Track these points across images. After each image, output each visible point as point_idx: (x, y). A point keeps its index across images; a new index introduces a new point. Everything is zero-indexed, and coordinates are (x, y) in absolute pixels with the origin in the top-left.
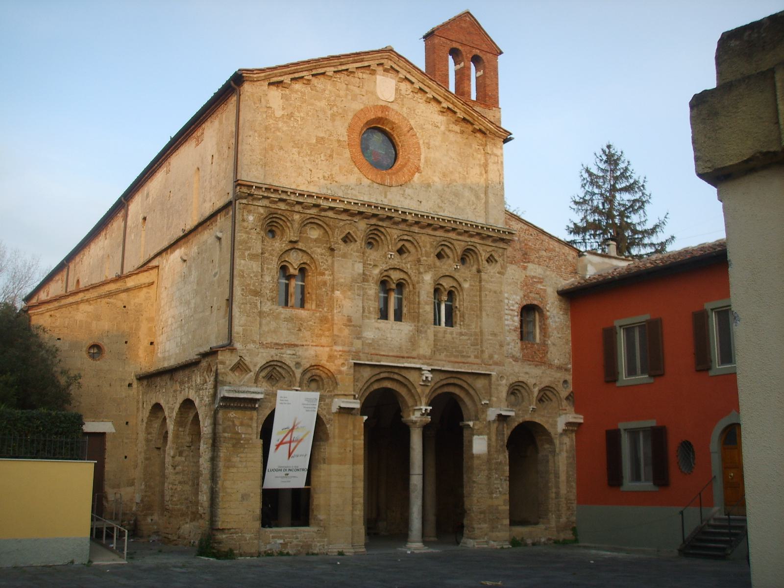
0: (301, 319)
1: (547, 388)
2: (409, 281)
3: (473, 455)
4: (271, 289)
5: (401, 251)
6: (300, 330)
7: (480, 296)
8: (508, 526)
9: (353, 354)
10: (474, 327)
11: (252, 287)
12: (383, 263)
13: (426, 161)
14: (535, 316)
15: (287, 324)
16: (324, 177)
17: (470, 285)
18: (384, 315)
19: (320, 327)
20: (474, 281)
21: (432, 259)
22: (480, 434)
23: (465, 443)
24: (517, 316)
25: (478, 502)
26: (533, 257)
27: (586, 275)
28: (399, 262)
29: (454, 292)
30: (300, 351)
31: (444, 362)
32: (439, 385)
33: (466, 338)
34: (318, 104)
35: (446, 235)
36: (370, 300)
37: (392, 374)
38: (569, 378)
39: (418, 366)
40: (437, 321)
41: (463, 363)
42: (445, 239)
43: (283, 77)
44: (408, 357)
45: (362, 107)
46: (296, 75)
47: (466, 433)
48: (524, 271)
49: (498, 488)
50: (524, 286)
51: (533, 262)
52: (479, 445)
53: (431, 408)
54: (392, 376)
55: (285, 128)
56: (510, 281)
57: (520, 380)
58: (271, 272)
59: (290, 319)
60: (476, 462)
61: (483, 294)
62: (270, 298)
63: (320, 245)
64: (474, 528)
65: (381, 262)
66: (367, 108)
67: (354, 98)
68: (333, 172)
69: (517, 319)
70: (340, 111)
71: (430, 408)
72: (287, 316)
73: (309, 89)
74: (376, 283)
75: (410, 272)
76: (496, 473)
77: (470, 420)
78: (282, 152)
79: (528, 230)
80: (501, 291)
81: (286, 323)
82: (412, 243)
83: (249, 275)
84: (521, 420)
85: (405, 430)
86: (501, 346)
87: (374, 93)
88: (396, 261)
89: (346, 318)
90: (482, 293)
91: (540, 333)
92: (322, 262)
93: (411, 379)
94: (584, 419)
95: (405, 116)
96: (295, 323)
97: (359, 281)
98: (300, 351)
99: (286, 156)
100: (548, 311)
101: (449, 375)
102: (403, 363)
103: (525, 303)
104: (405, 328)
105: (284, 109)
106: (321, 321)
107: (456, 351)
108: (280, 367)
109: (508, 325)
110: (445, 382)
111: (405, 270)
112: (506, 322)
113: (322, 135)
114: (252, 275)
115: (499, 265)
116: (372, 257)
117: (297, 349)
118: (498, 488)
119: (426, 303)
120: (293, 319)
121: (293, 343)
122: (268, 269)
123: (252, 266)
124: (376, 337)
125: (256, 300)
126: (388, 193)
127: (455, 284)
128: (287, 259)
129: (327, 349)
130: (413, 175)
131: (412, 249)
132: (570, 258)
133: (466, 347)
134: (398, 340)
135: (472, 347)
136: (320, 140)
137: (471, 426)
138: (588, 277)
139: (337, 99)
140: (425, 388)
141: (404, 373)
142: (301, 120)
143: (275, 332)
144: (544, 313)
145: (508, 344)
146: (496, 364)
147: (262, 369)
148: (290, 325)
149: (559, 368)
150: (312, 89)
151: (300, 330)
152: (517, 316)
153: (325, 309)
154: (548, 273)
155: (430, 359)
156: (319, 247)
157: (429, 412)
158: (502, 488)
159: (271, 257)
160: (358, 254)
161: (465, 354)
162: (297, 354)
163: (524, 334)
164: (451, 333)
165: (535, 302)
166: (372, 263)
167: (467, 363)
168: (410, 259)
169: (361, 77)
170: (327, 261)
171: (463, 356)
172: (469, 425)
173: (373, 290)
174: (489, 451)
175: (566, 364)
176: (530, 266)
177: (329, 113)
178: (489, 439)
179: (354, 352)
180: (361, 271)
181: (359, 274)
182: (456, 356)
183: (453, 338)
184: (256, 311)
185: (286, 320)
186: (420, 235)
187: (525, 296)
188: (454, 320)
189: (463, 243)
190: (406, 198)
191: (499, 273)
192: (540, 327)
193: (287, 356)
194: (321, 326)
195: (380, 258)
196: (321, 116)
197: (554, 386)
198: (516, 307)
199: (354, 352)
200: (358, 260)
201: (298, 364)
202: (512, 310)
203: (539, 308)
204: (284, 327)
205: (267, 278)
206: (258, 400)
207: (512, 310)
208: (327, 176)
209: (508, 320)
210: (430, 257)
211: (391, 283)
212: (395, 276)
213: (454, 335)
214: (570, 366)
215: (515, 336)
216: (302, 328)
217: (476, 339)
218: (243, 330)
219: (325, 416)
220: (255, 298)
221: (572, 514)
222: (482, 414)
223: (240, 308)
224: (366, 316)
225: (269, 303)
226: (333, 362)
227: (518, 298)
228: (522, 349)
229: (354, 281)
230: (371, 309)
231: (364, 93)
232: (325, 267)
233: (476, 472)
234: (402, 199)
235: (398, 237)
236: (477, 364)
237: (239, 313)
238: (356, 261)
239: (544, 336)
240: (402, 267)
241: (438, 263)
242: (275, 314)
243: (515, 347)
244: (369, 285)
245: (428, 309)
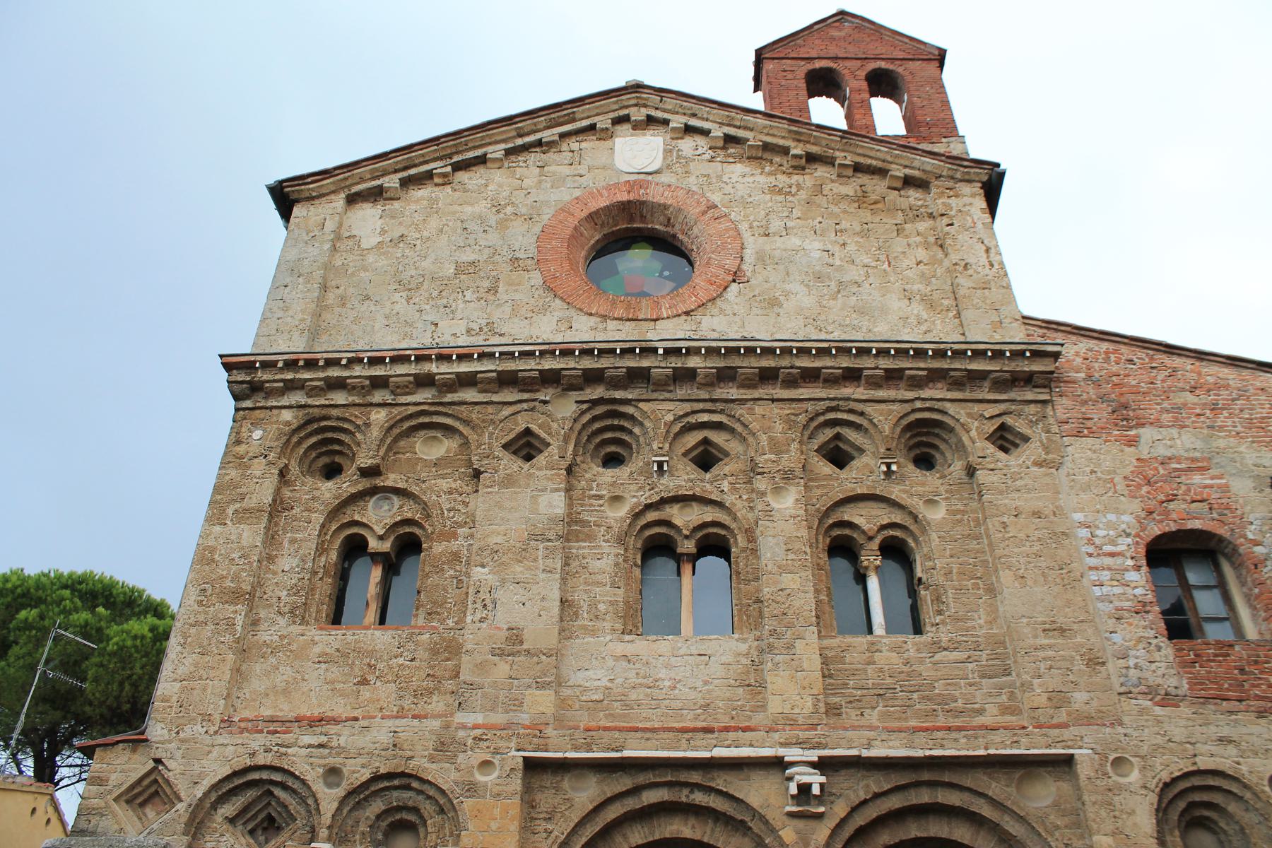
0: (371, 653)
2: (733, 526)
6: (364, 682)
30: (344, 737)
32: (872, 812)
35: (833, 393)
37: (686, 791)
42: (834, 404)
54: (684, 796)
62: (286, 610)
72: (328, 650)
75: (729, 500)
81: (323, 666)
82: (732, 431)
88: (684, 478)
93: (754, 800)
96: (352, 666)
98: (344, 737)
111: (713, 497)
117: (333, 729)
120: (347, 656)
124: (620, 681)
128: (357, 517)
134: (699, 684)
140: (812, 824)
141: (721, 781)
148: (335, 672)
162: (334, 744)
168: (727, 469)
185: (324, 659)
186: (749, 405)
204: (315, 677)
211: (679, 539)
212: (685, 518)
216: (371, 677)
236: (1005, 728)
242: (294, 647)
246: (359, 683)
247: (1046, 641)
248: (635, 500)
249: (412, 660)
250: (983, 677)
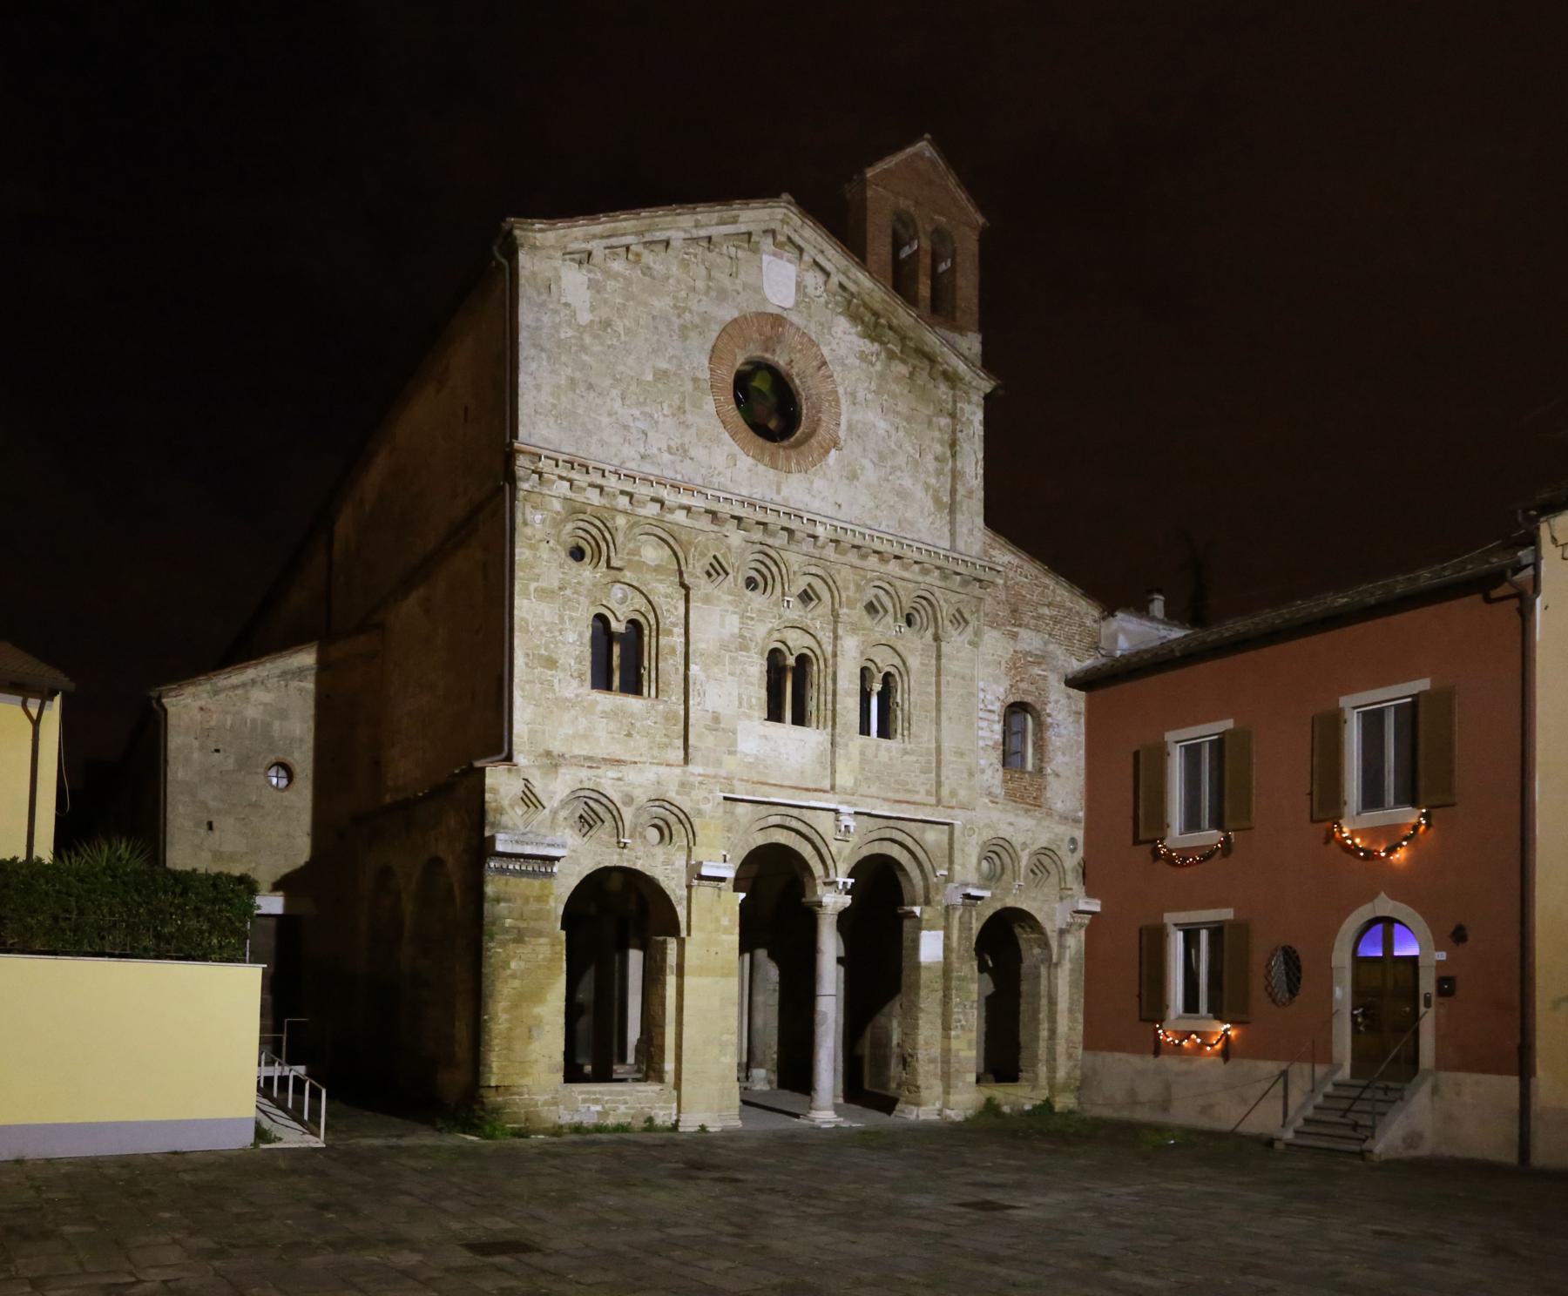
0: (632, 715)
1: (1043, 851)
3: (919, 963)
4: (578, 657)
5: (806, 597)
6: (629, 735)
7: (938, 684)
8: (974, 1084)
9: (723, 780)
10: (926, 739)
11: (543, 652)
12: (775, 617)
14: (1025, 719)
15: (607, 724)
16: (669, 448)
17: (922, 664)
18: (775, 714)
19: (664, 732)
20: (928, 656)
21: (859, 612)
22: (931, 928)
23: (907, 943)
24: (999, 722)
25: (927, 1043)
26: (1026, 619)
27: (1115, 650)
28: (800, 616)
29: (893, 676)
31: (874, 801)
33: (913, 758)
34: (656, 303)
36: (752, 684)
39: (832, 806)
40: (865, 730)
41: (908, 802)
43: (591, 243)
44: (816, 790)
45: (736, 314)
46: (613, 241)
47: (907, 924)
48: (1012, 642)
49: (960, 1021)
50: (1010, 669)
51: (1027, 626)
52: (930, 947)
53: (853, 880)
55: (597, 348)
56: (989, 657)
57: (1000, 836)
58: (576, 624)
59: (613, 714)
60: (924, 975)
61: (944, 679)
63: (662, 577)
64: (918, 1087)
65: (770, 615)
66: (745, 318)
67: (722, 296)
68: (686, 440)
69: (998, 727)
70: (697, 320)
71: (851, 881)
73: (639, 272)
74: (762, 654)
75: (820, 635)
76: (958, 996)
77: (914, 904)
78: (592, 394)
79: (1021, 567)
80: (973, 675)
83: (537, 628)
85: (809, 917)
86: (971, 775)
87: (758, 289)
88: (795, 612)
89: (710, 715)
90: (942, 677)
91: (1033, 755)
92: (668, 611)
94: (1102, 907)
97: (732, 647)
99: (599, 401)
100: (1049, 715)
101: (885, 822)
102: (808, 800)
103: (1011, 700)
104: (810, 739)
105: (593, 309)
106: (667, 719)
107: (896, 781)
109: (983, 738)
110: (875, 835)
112: (981, 733)
113: (664, 365)
114: (543, 629)
115: (970, 629)
116: (755, 605)
118: (960, 1021)
119: (847, 693)
120: (616, 714)
121: (618, 758)
122: (571, 619)
123: (543, 611)
125: (552, 676)
126: (783, 486)
127: (897, 661)
129: (678, 771)
131: (826, 595)
132: (1089, 622)
133: (913, 774)
135: (923, 775)
136: (661, 375)
137: (918, 914)
138: (1118, 653)
139: (691, 295)
142: (626, 334)
143: (585, 737)
144: (1042, 718)
145: (983, 771)
146: (963, 807)
147: (564, 804)
148: (612, 726)
150: (644, 274)
151: (629, 735)
152: (999, 722)
153: (673, 698)
154: (1051, 647)
155: (853, 795)
157: (849, 887)
158: (967, 1021)
160: (731, 598)
161: (910, 787)
163: (1010, 756)
164: (888, 749)
165: (1028, 699)
166: (754, 615)
167: (914, 803)
168: (820, 610)
169: (733, 255)
170: (676, 608)
171: (909, 791)
172: (913, 912)
173: (757, 669)
174: (946, 958)
176: (1023, 633)
177: (676, 322)
178: (947, 937)
179: (725, 778)
180: (736, 630)
181: (732, 635)
182: (898, 791)
183: (891, 759)
184: (550, 696)
185: (605, 714)
187: (1012, 686)
188: (892, 727)
189: (911, 586)
190: (813, 496)
191: (970, 643)
192: (1034, 743)
193: (607, 781)
194: (666, 729)
195: (768, 607)
196: (662, 328)
198: (997, 707)
199: (725, 778)
200: (731, 608)
202: (990, 711)
203: (1033, 708)
204: (602, 729)
205: (571, 637)
206: (558, 859)
207: (990, 711)
208: (674, 447)
209: (982, 729)
210: (855, 608)
213: (894, 753)
215: (995, 757)
217: (929, 762)
218: (530, 731)
220: (550, 673)
221: (1075, 1066)
222: (937, 894)
223: (523, 690)
224: (745, 713)
225: (575, 683)
226: (688, 794)
227: (1000, 690)
228: (1005, 781)
229: (724, 646)
230: (754, 700)
231: (740, 289)
232: (672, 619)
233: (923, 993)
234: (807, 498)
235: (800, 567)
237: (521, 699)
238: (727, 611)
239: (1041, 760)
240: (807, 625)
241: (867, 620)
242: (585, 704)
243: (993, 778)
244: (748, 657)
245: (850, 705)
246: (626, 735)
247: (953, 759)
248: (771, 625)
249: (655, 723)
250: (921, 772)
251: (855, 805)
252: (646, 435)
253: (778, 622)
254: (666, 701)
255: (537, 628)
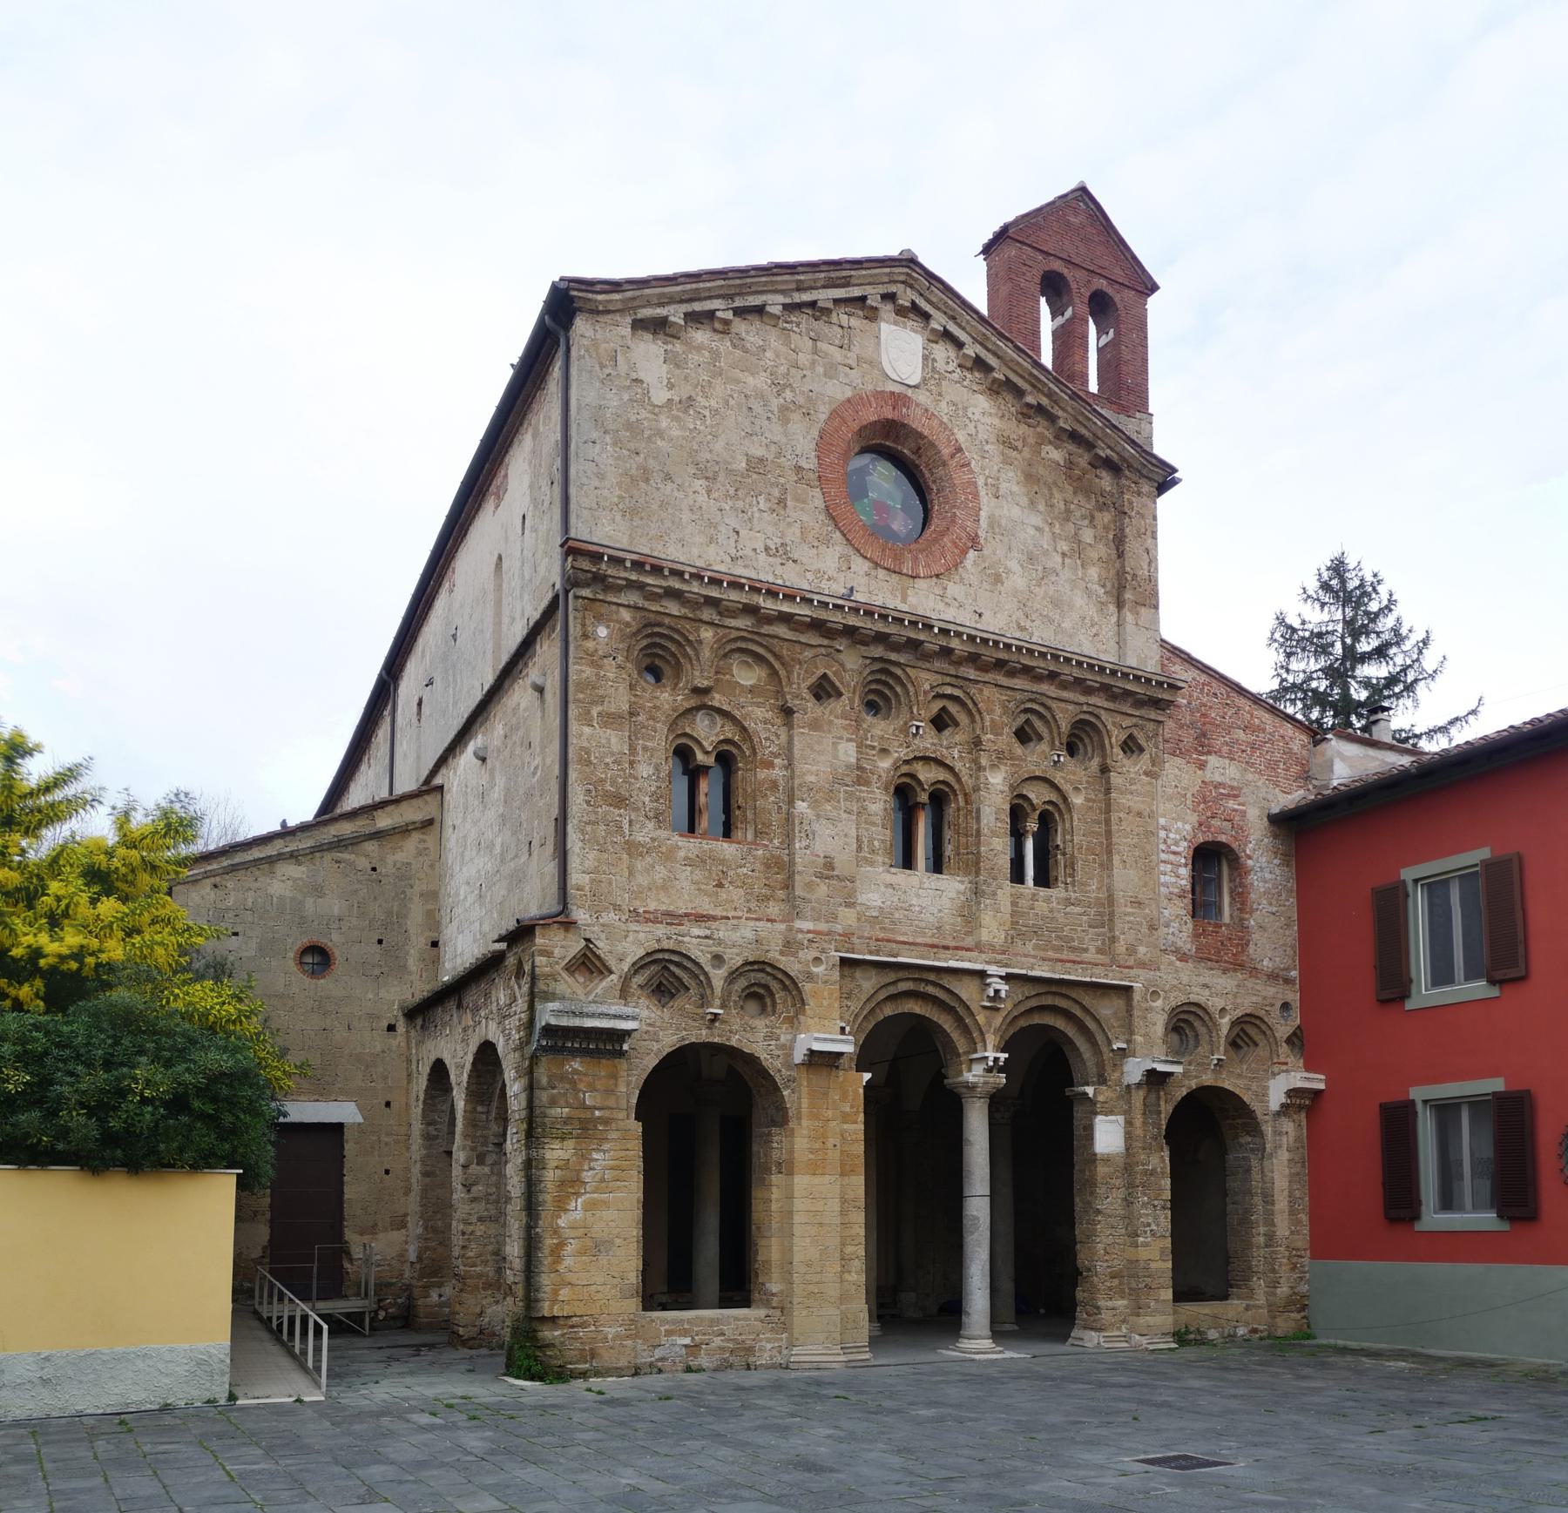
0: (723, 862)
6: (720, 885)
13: (991, 525)
15: (692, 872)
16: (767, 549)
36: (874, 824)
38: (1294, 997)
40: (1018, 876)
44: (957, 948)
47: (1079, 1112)
52: (1108, 1136)
53: (1007, 1055)
56: (1170, 791)
62: (651, 814)
65: (896, 744)
71: (1003, 1056)
75: (958, 766)
84: (1193, 1084)
85: (951, 1106)
86: (1153, 928)
88: (928, 741)
89: (821, 861)
95: (945, 420)
97: (848, 780)
100: (1250, 857)
102: (946, 960)
104: (951, 886)
106: (768, 866)
107: (1057, 936)
108: (678, 964)
109: (1166, 885)
120: (704, 861)
122: (645, 749)
127: (1054, 797)
129: (782, 927)
130: (964, 552)
137: (1091, 1096)
141: (946, 981)
146: (1142, 965)
147: (638, 967)
148: (698, 875)
149: (1273, 977)
152: (1186, 865)
156: (758, 705)
159: (651, 722)
163: (1202, 903)
175: (1287, 969)
179: (840, 935)
180: (853, 760)
185: (689, 862)
188: (1053, 874)
189: (1071, 707)
190: (947, 604)
191: (1146, 774)
193: (694, 942)
194: (767, 878)
197: (1262, 1013)
199: (840, 935)
201: (718, 959)
208: (773, 547)
210: (1002, 734)
214: (1294, 973)
219: (780, 1071)
220: (617, 812)
222: (1113, 1071)
225: (650, 825)
226: (795, 955)
228: (1196, 936)
229: (838, 780)
234: (941, 606)
238: (841, 738)
241: (1018, 749)
242: (664, 849)
245: (998, 847)
251: (1006, 966)
252: (738, 533)
253: (905, 751)
254: (766, 846)
255: (601, 759)
